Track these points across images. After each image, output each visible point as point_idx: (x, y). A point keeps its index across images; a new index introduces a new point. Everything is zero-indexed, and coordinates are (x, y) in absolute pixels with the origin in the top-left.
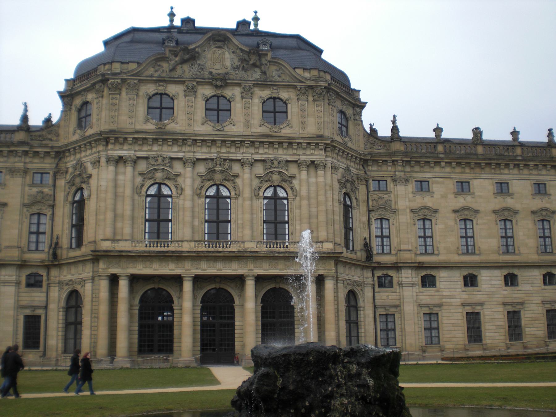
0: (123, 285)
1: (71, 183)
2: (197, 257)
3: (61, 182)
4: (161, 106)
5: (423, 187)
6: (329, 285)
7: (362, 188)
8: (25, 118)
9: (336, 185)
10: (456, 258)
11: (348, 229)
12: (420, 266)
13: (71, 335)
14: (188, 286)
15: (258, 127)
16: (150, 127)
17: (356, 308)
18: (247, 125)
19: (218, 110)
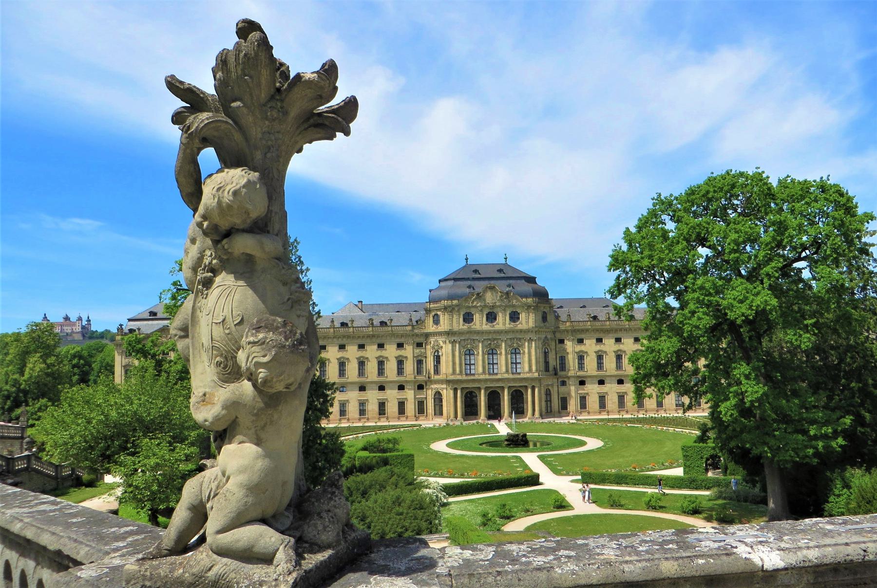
0: (459, 392)
1: (433, 348)
2: (486, 380)
3: (428, 347)
4: (468, 318)
5: (581, 341)
6: (536, 390)
7: (553, 343)
8: (411, 320)
9: (541, 346)
10: (595, 373)
11: (547, 363)
12: (579, 377)
13: (437, 408)
14: (483, 392)
15: (508, 325)
16: (465, 327)
17: (550, 394)
18: (504, 324)
19: (491, 317)
